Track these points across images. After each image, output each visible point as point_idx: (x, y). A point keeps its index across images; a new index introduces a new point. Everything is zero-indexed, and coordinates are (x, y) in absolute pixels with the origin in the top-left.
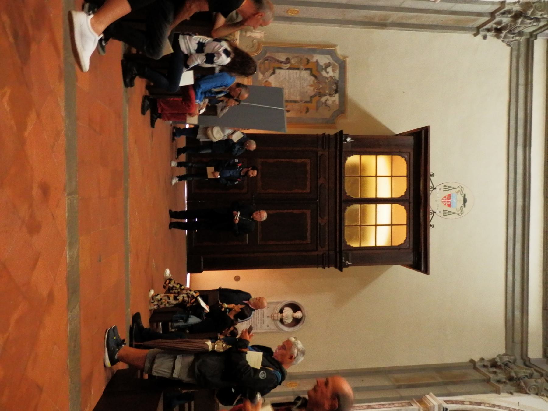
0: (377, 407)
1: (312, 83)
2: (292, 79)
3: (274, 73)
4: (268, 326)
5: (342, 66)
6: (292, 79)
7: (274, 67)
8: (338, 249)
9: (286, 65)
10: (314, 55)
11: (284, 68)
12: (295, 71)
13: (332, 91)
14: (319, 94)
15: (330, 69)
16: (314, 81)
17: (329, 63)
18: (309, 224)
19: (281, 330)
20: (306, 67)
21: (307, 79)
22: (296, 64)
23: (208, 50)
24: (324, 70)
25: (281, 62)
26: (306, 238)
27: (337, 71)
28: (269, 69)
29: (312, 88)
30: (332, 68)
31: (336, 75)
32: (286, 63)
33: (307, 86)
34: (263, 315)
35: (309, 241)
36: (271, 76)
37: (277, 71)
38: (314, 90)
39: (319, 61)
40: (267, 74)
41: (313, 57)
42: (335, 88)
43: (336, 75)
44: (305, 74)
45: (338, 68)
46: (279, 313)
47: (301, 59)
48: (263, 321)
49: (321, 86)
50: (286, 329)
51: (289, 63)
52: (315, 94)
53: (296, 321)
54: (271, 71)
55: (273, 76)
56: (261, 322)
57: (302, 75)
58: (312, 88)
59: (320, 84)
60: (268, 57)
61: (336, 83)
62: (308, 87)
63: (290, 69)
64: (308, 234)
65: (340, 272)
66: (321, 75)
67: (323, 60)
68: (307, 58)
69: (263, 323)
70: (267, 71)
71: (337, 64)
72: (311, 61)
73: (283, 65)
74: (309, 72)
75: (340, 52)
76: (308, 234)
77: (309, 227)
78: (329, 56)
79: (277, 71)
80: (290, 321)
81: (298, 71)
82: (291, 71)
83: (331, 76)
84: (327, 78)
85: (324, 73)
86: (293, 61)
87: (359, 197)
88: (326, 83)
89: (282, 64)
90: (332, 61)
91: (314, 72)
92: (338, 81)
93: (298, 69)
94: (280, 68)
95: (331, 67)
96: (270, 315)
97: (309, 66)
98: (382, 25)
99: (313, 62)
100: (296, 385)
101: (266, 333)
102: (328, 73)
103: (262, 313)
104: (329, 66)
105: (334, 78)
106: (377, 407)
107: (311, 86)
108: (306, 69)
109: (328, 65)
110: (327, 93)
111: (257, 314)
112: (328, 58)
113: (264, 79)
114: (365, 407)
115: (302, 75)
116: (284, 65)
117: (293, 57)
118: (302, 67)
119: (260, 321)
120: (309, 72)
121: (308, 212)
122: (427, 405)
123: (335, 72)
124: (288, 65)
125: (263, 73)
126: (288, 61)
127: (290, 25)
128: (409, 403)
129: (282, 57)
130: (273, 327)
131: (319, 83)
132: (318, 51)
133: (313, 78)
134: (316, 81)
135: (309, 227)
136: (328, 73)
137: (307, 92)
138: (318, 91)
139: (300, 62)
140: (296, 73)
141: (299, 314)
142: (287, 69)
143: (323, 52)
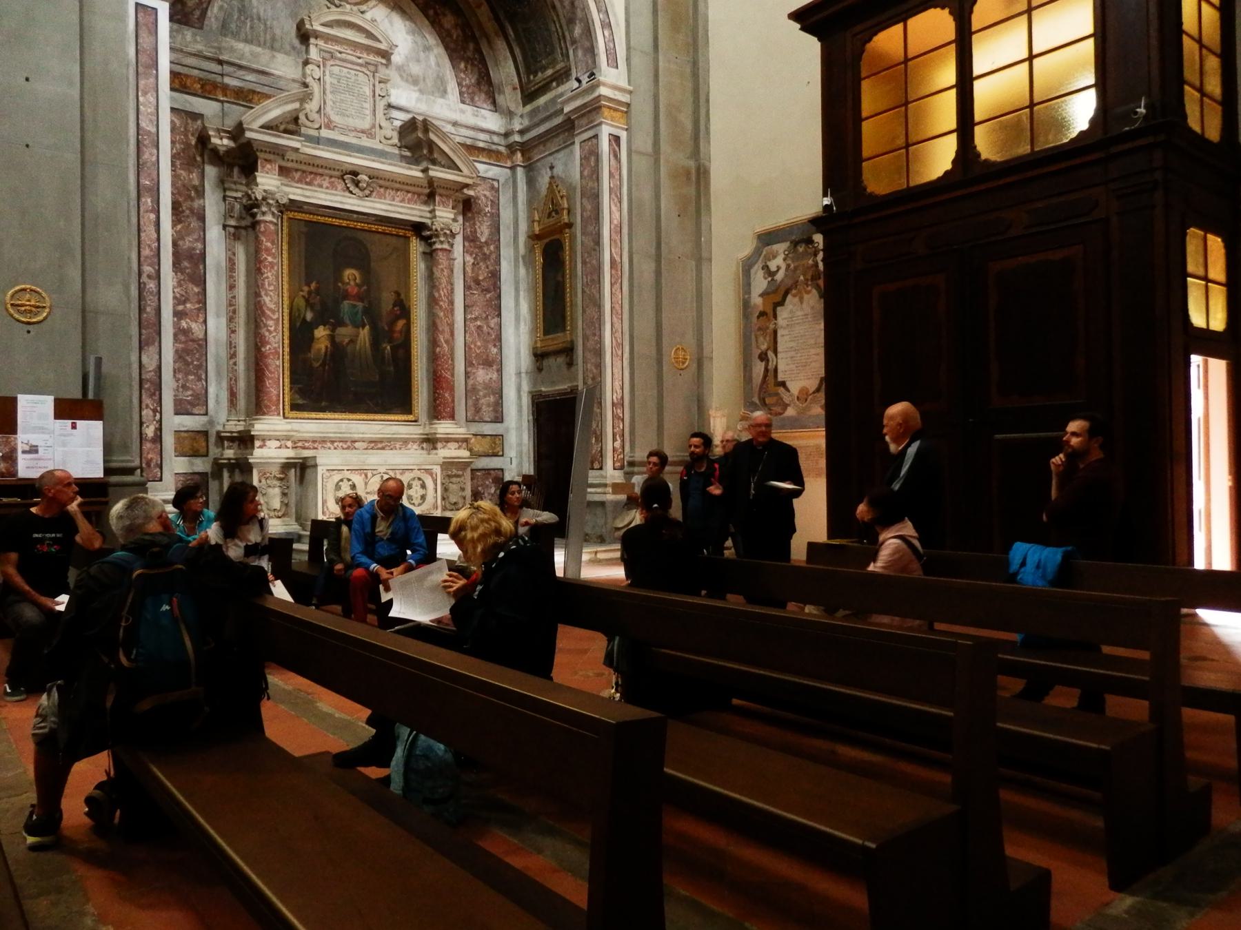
1: (797, 299)
2: (793, 344)
5: (767, 238)
6: (793, 344)
7: (775, 385)
9: (771, 360)
10: (752, 304)
11: (775, 363)
12: (779, 339)
13: (809, 250)
14: (816, 279)
15: (773, 265)
16: (794, 296)
17: (763, 269)
20: (772, 318)
21: (791, 312)
22: (768, 339)
24: (775, 278)
25: (766, 370)
27: (776, 247)
28: (777, 394)
29: (806, 297)
30: (770, 260)
31: (781, 248)
32: (768, 361)
33: (802, 309)
36: (789, 391)
37: (781, 377)
38: (808, 292)
39: (761, 292)
40: (786, 399)
41: (755, 305)
42: (803, 245)
43: (781, 248)
44: (783, 314)
45: (769, 247)
47: (760, 329)
49: (802, 278)
52: (817, 290)
54: (781, 390)
55: (788, 384)
57: (784, 325)
58: (806, 297)
59: (797, 281)
60: (760, 399)
61: (795, 244)
62: (804, 305)
63: (775, 352)
66: (782, 281)
67: (760, 283)
68: (758, 317)
70: (782, 399)
71: (764, 253)
72: (761, 308)
73: (771, 366)
75: (747, 249)
78: (753, 271)
79: (781, 377)
81: (779, 333)
82: (779, 349)
84: (788, 266)
85: (780, 276)
88: (796, 268)
89: (769, 367)
90: (759, 265)
91: (778, 298)
92: (791, 242)
93: (775, 332)
94: (776, 370)
95: (769, 263)
97: (770, 312)
98: (698, 177)
99: (764, 301)
102: (779, 268)
104: (768, 267)
105: (786, 253)
107: (801, 300)
108: (775, 317)
110: (813, 261)
112: (756, 273)
113: (795, 403)
115: (784, 325)
116: (770, 364)
117: (758, 347)
118: (772, 326)
123: (777, 251)
124: (770, 354)
125: (786, 406)
126: (763, 357)
127: (715, 362)
129: (759, 368)
131: (796, 283)
132: (746, 296)
133: (789, 297)
134: (794, 292)
136: (779, 268)
137: (812, 308)
138: (810, 283)
139: (762, 329)
140: (783, 336)
142: (776, 356)
143: (747, 286)
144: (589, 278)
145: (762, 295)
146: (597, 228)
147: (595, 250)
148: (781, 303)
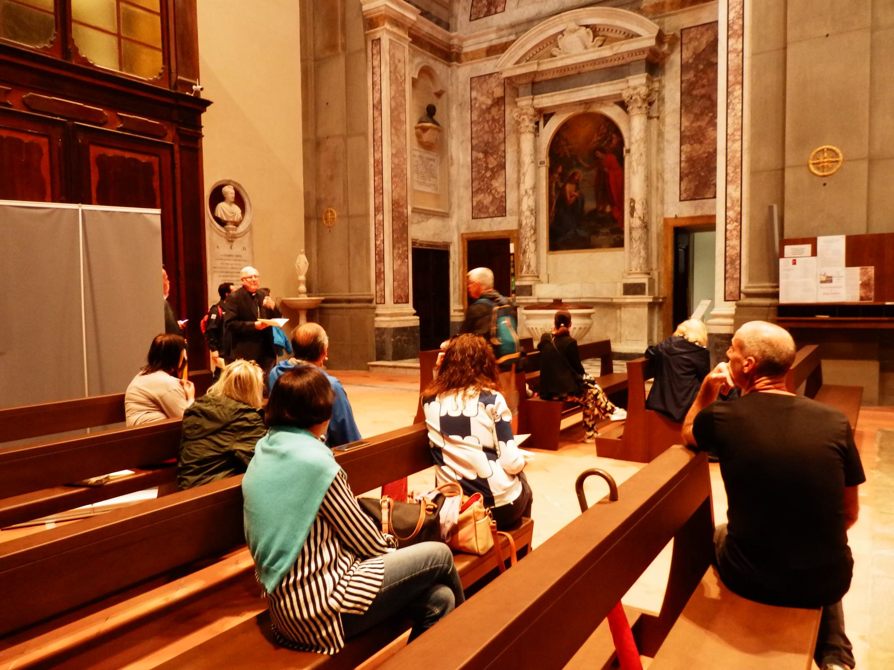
0: (377, 95)
4: (244, 249)
8: (172, 102)
18: (119, 153)
19: (250, 228)
23: (490, 439)
26: (149, 165)
34: (229, 256)
35: (154, 160)
46: (226, 227)
48: (238, 256)
50: (248, 217)
53: (239, 200)
56: (239, 260)
64: (143, 159)
65: (212, 105)
69: (240, 256)
76: (143, 159)
77: (128, 155)
80: (237, 209)
87: (53, 17)
96: (228, 246)
100: (331, 211)
101: (253, 253)
103: (227, 258)
106: (377, 95)
111: (226, 266)
114: (377, 114)
119: (238, 262)
121: (95, 151)
122: (381, 15)
128: (373, 41)
130: (245, 240)
135: (128, 155)
141: (229, 191)
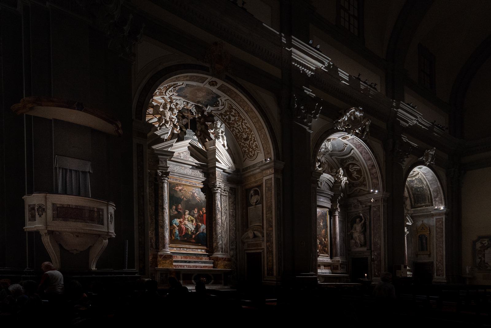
3: (487, 263)
25: (481, 261)
27: (486, 239)
37: (486, 262)
51: (481, 258)
74: (485, 250)
79: (486, 262)
81: (486, 254)
83: (488, 242)
84: (488, 243)
86: (480, 256)
93: (484, 254)
94: (484, 261)
108: (484, 251)
109: (482, 243)
118: (483, 253)
120: (485, 250)
136: (485, 243)
144: (439, 243)
145: (480, 247)
146: (442, 234)
147: (441, 238)
148: (487, 249)
